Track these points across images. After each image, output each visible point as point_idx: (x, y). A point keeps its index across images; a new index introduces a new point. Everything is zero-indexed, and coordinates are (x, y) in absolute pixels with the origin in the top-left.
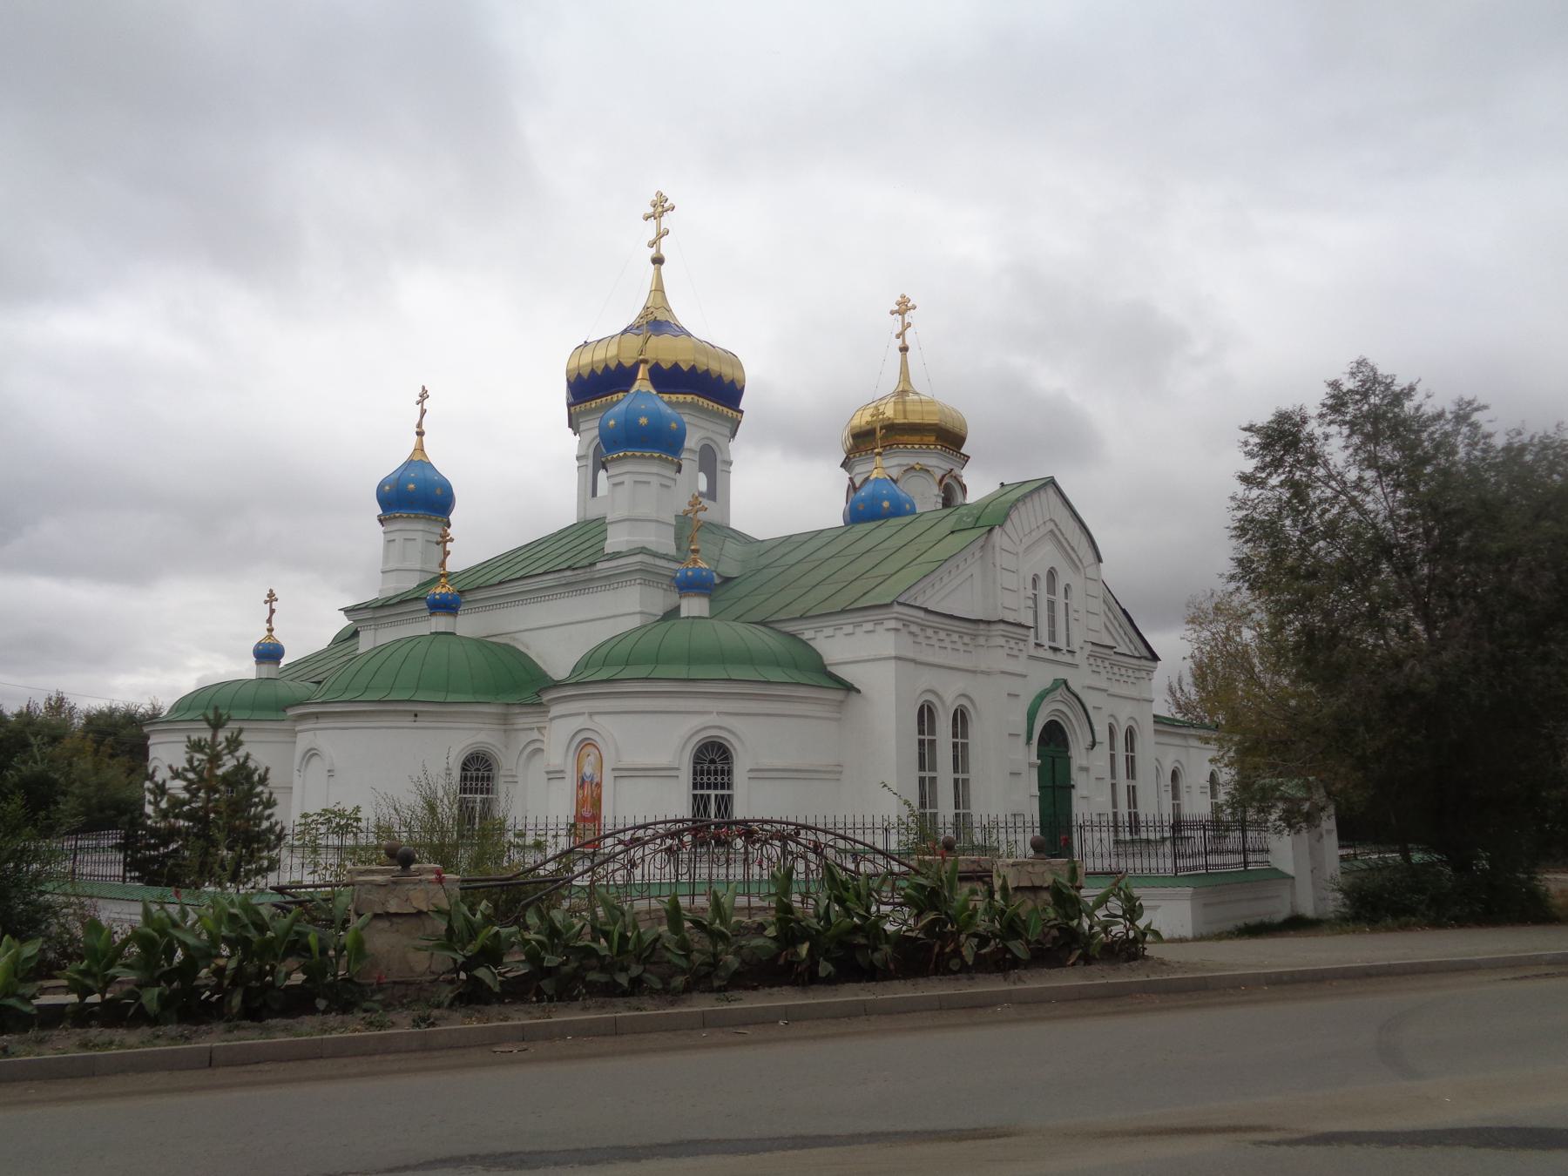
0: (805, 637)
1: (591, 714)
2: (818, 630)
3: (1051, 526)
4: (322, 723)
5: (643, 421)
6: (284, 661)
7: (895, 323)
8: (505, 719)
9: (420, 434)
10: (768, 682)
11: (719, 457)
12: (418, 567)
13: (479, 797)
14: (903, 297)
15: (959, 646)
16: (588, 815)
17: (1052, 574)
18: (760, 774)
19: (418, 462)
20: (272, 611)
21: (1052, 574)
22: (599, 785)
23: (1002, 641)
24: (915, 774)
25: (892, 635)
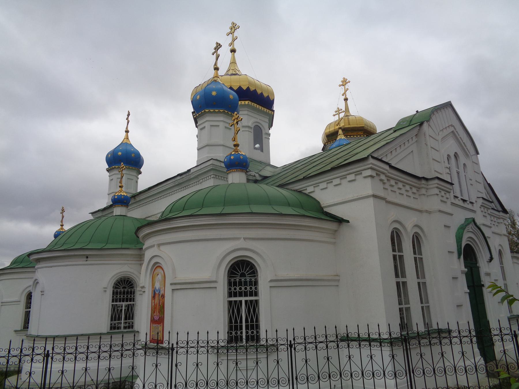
0: (307, 192)
2: (316, 185)
3: (452, 129)
7: (342, 90)
9: (127, 132)
10: (281, 215)
11: (263, 132)
13: (124, 304)
14: (344, 78)
15: (410, 194)
16: (156, 318)
17: (456, 155)
18: (278, 283)
19: (126, 144)
20: (63, 217)
21: (456, 155)
22: (163, 296)
23: (436, 191)
24: (393, 280)
25: (369, 180)
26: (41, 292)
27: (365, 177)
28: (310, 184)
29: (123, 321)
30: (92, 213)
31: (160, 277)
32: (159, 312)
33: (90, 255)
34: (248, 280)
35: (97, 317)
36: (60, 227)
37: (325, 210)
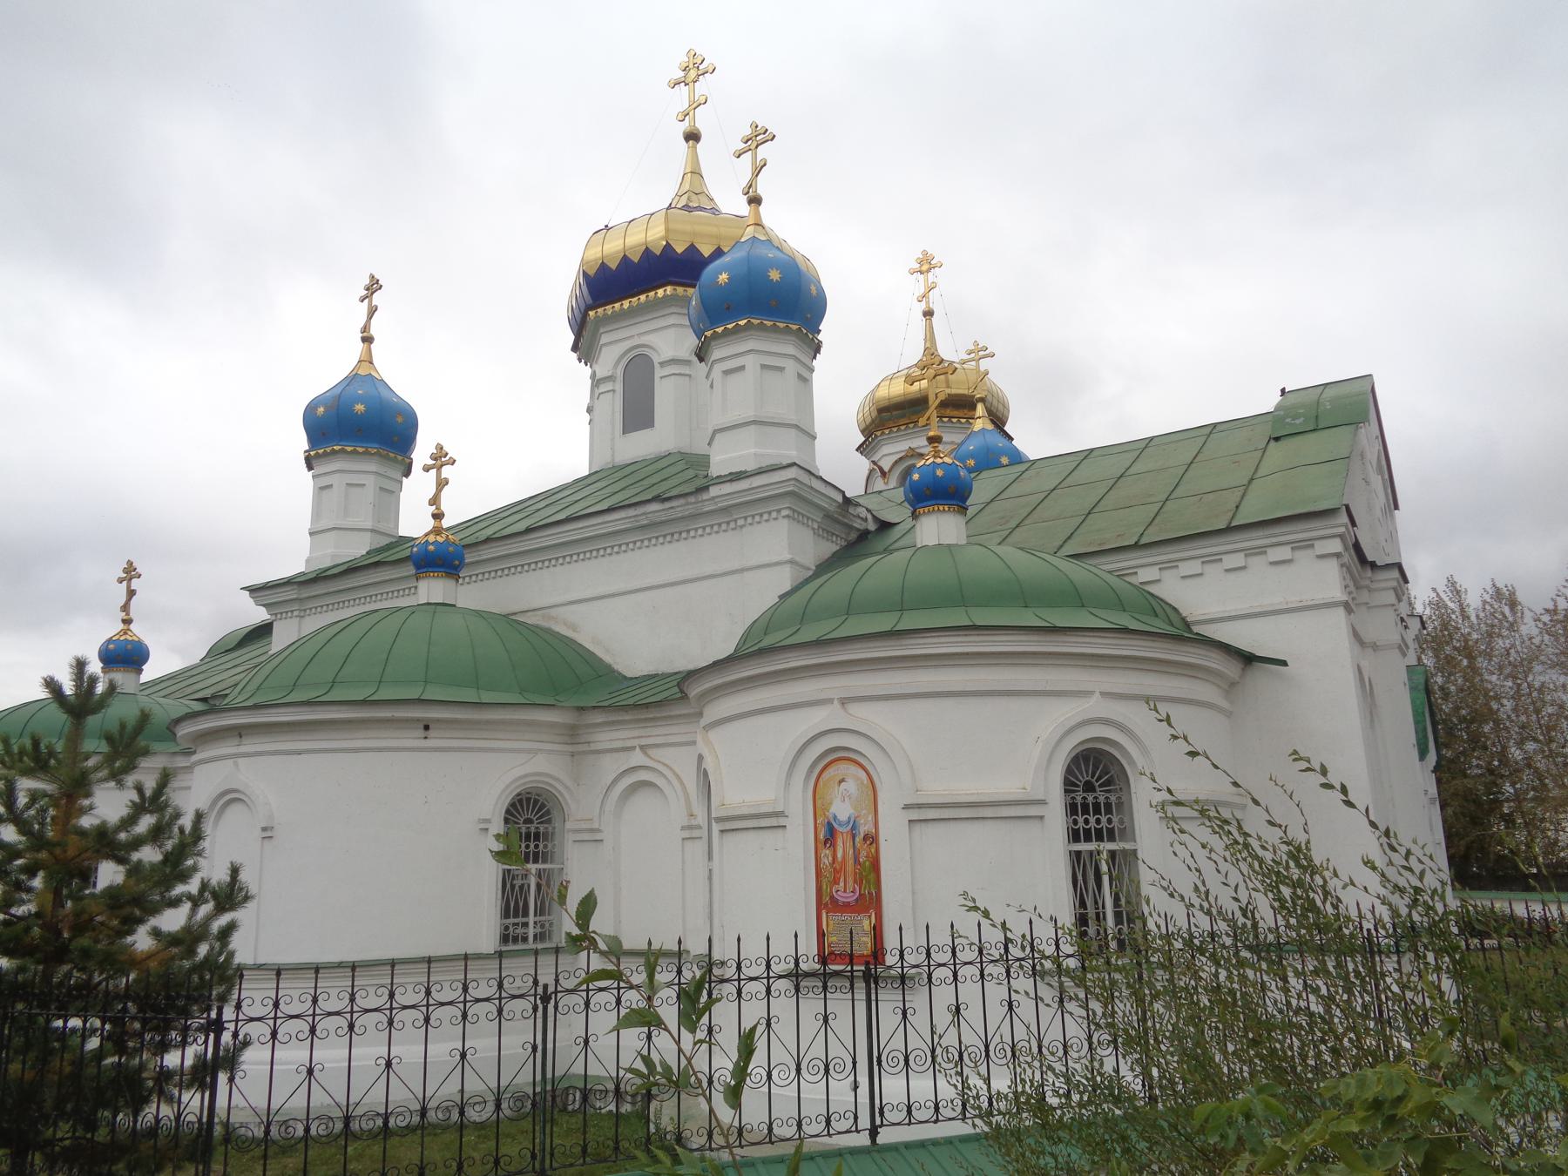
1: (844, 702)
2: (1171, 565)
4: (249, 746)
5: (775, 275)
6: (150, 672)
7: (917, 285)
8: (572, 734)
9: (367, 340)
12: (369, 524)
13: (532, 867)
14: (925, 253)
19: (363, 378)
20: (131, 593)
22: (872, 839)
26: (264, 829)
27: (1321, 557)
28: (1151, 560)
29: (531, 919)
30: (254, 591)
31: (850, 786)
32: (859, 880)
33: (438, 720)
34: (1102, 799)
35: (461, 906)
36: (121, 626)
37: (1196, 629)
